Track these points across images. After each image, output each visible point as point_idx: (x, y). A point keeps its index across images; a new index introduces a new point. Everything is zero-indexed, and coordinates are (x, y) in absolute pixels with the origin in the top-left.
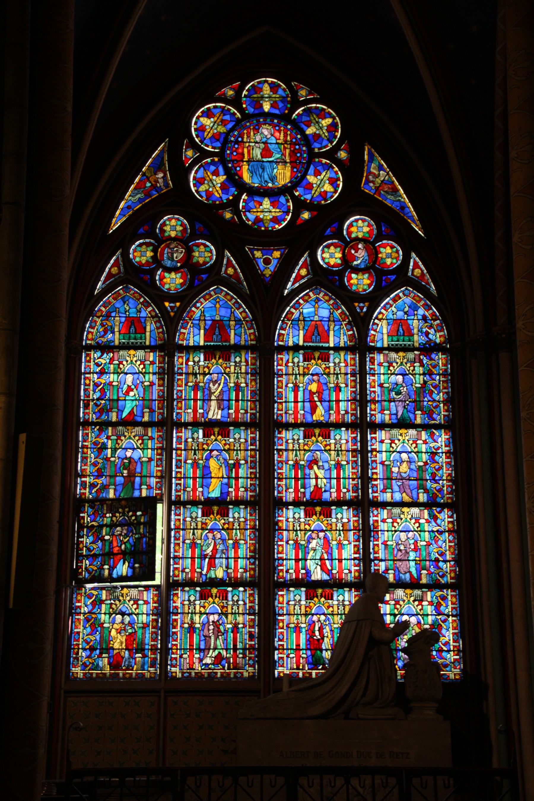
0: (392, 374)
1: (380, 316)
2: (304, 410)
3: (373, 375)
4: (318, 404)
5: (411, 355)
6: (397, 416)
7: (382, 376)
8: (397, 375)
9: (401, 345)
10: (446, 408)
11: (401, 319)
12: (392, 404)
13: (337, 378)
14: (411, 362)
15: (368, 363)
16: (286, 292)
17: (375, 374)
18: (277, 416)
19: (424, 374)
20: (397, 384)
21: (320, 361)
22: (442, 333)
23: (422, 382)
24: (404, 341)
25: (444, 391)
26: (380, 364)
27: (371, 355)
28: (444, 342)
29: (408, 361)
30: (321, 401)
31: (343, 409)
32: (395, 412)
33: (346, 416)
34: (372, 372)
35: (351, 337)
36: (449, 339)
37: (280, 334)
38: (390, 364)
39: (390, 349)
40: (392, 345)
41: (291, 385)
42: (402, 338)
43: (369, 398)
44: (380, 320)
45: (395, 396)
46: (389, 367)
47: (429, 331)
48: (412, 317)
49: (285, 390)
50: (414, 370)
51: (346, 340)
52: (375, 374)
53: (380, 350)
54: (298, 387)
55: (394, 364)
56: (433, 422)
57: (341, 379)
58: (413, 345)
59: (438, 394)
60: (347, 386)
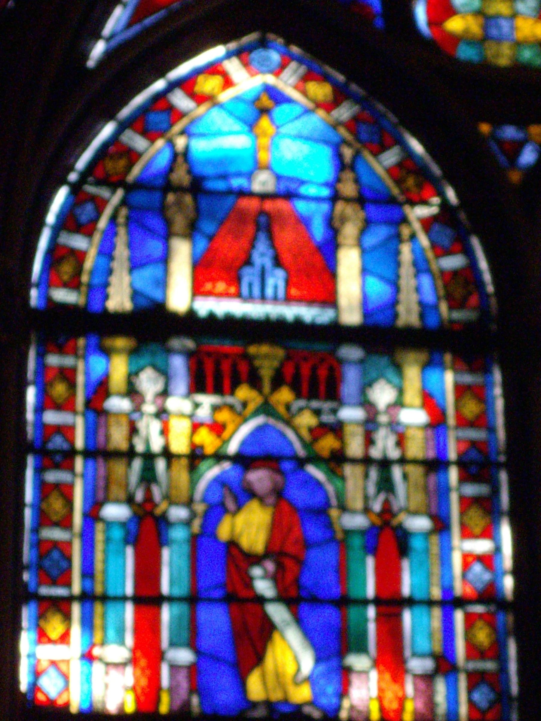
2: (193, 644)
4: (278, 613)
13: (386, 485)
16: (99, 49)
18: (37, 674)
21: (285, 395)
30: (294, 598)
31: (423, 645)
33: (441, 688)
35: (461, 285)
37: (56, 254)
41: (115, 511)
49: (88, 538)
51: (429, 297)
54: (163, 522)
57: (406, 489)
60: (441, 525)
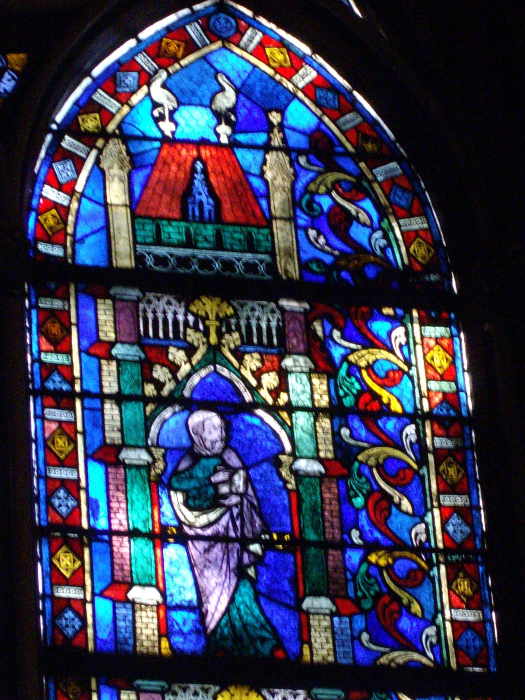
0: (162, 402)
1: (90, 123)
3: (64, 400)
5: (264, 317)
6: (202, 616)
7: (110, 410)
8: (190, 405)
9: (206, 263)
10: (464, 586)
11: (204, 142)
12: (174, 552)
14: (264, 349)
15: (33, 339)
17: (72, 395)
19: (336, 411)
20: (191, 452)
22: (417, 223)
23: (327, 451)
24: (219, 245)
25: (448, 500)
26: (98, 350)
27: (45, 303)
28: (431, 266)
29: (247, 340)
32: (190, 595)
34: (55, 382)
36: (457, 248)
38: (153, 354)
39: (146, 277)
40: (160, 260)
42: (209, 230)
43: (40, 515)
44: (88, 139)
45: (188, 516)
46: (146, 367)
47: (351, 208)
48: (261, 138)
50: (283, 386)
52: (72, 395)
53: (100, 281)
55: (177, 355)
56: (400, 657)
58: (272, 267)
59: (419, 514)
